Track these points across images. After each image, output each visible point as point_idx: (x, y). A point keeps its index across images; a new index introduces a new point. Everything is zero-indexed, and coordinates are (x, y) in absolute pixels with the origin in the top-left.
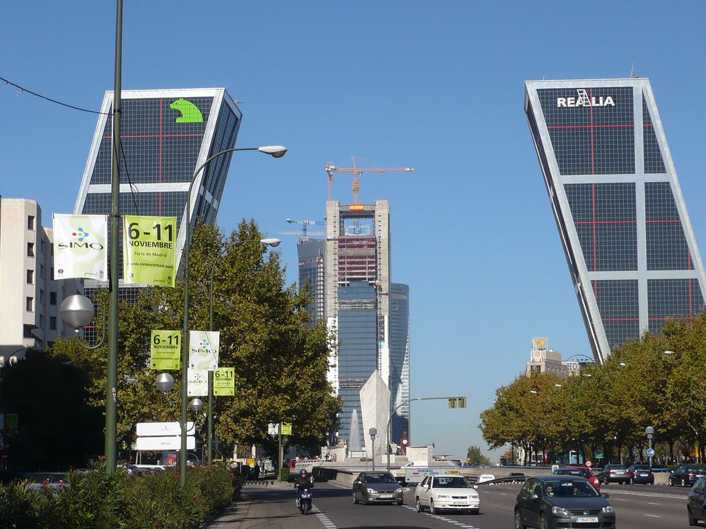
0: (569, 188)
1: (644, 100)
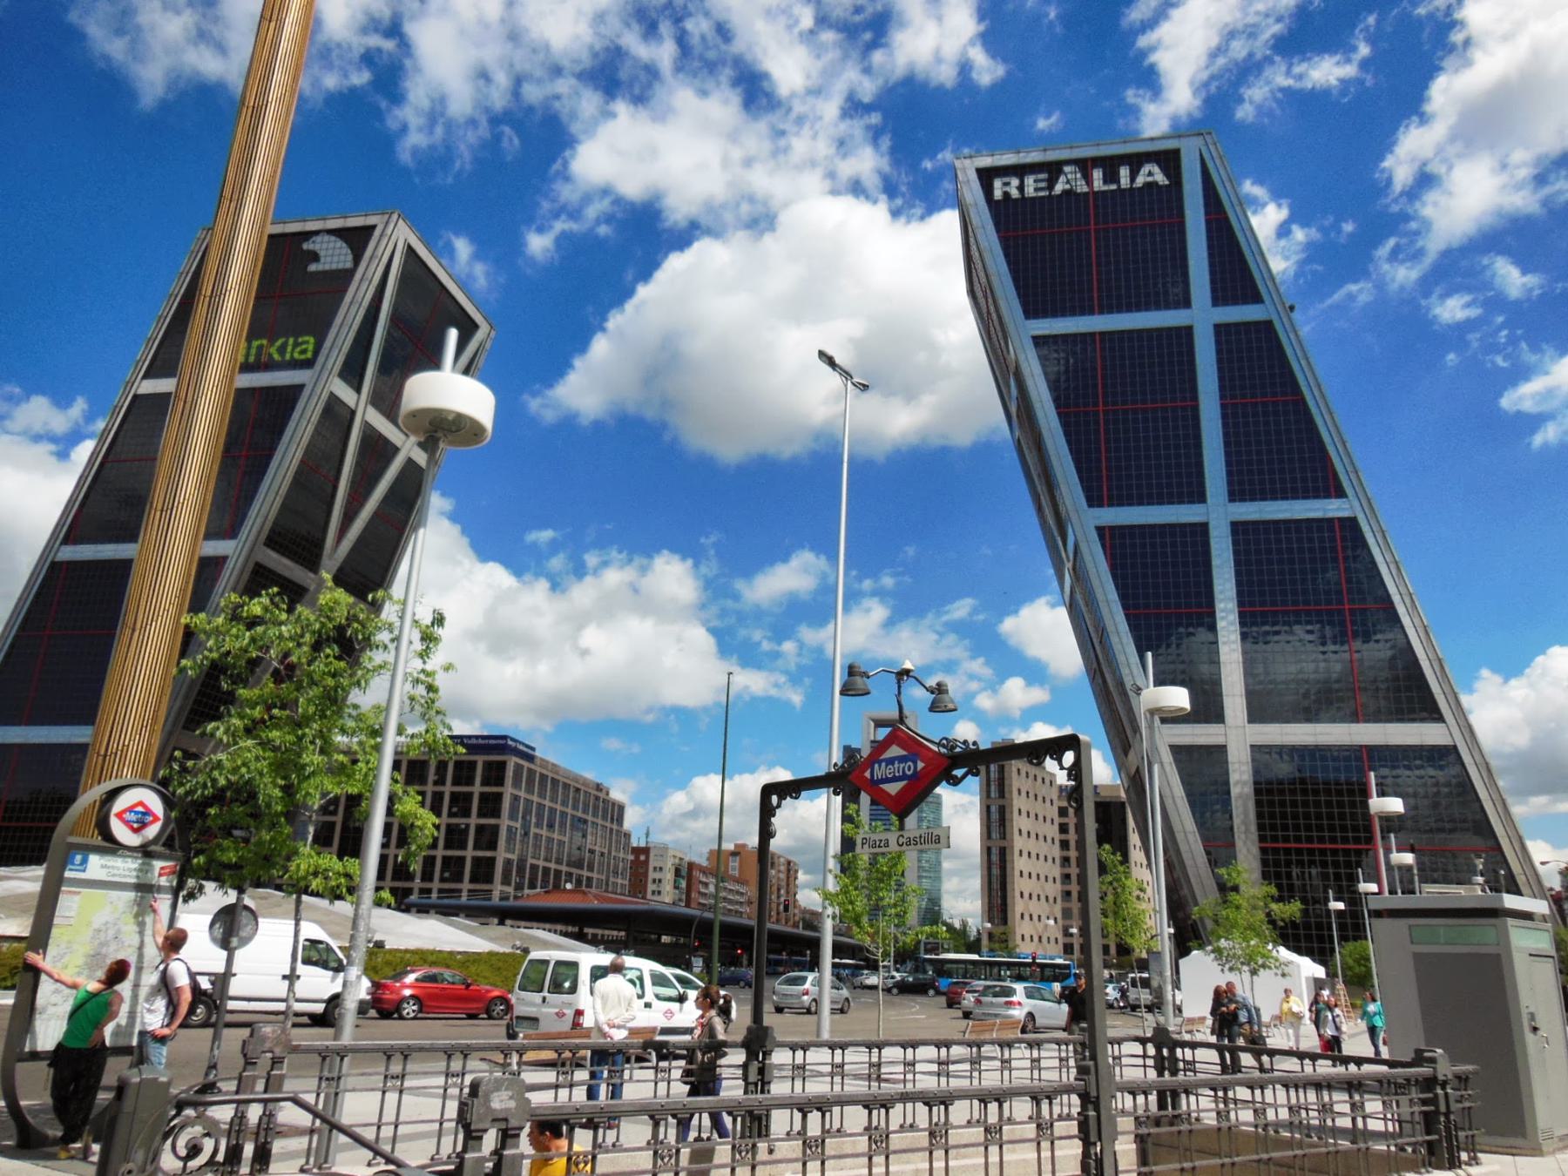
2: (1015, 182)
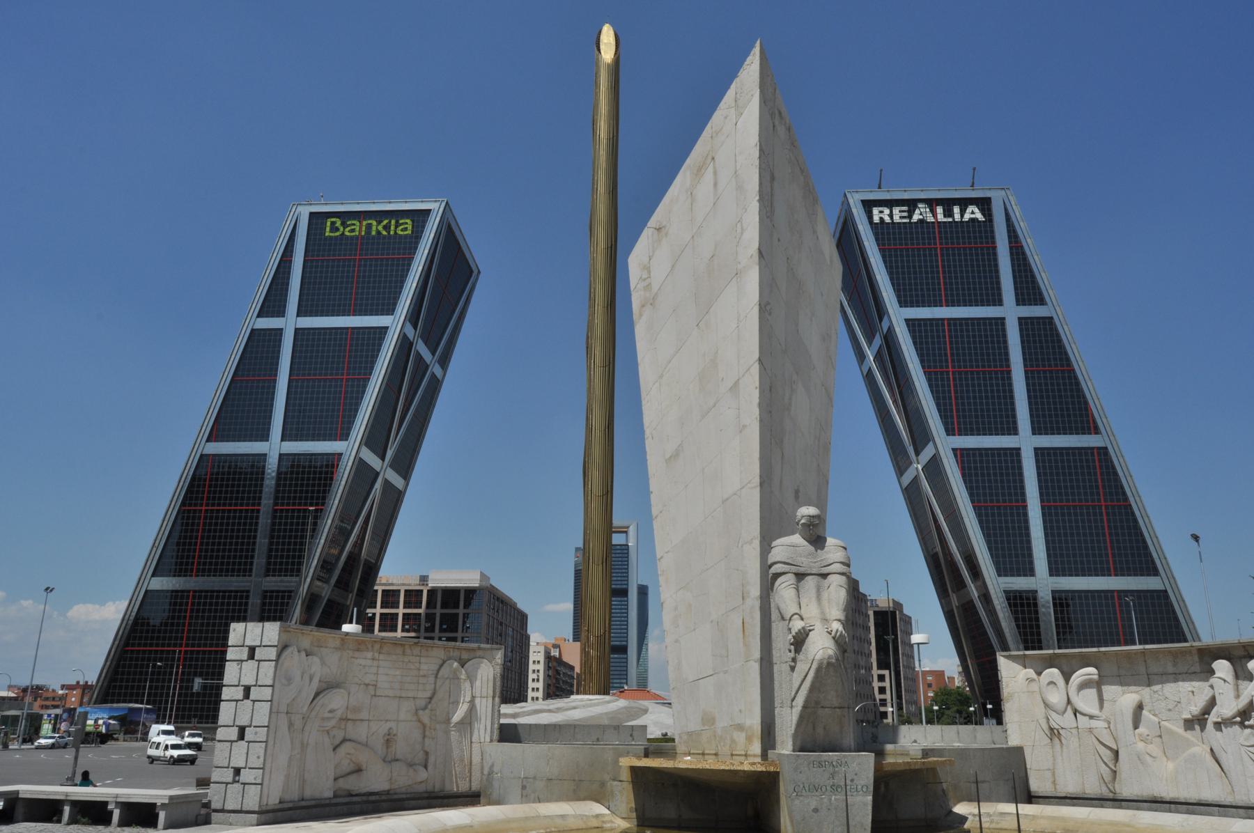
0: (911, 324)
1: (1006, 209)
2: (887, 211)
